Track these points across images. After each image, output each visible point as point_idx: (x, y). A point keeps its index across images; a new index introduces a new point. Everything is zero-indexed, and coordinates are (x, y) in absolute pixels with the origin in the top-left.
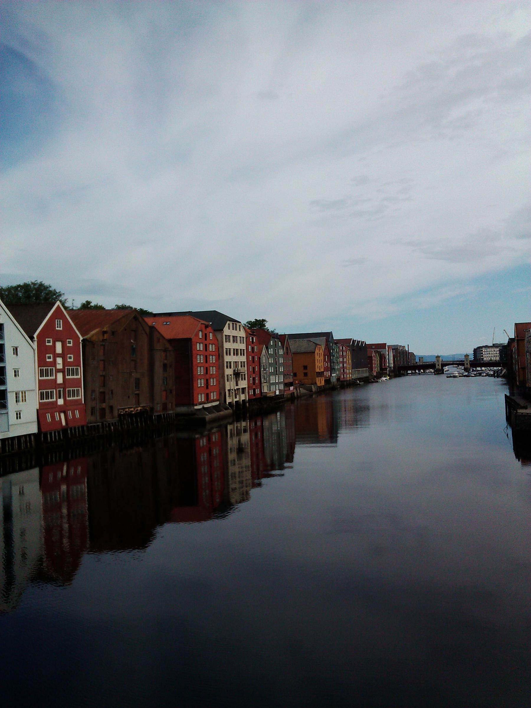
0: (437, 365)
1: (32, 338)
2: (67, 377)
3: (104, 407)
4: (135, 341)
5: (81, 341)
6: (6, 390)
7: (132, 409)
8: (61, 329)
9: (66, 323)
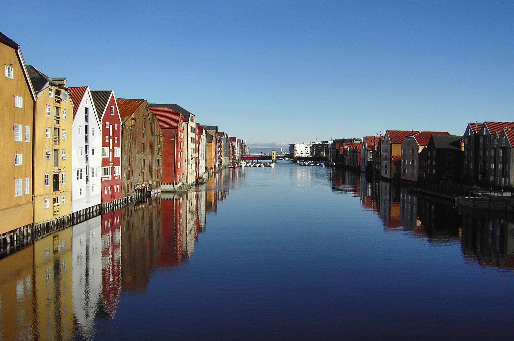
0: (272, 157)
1: (100, 121)
2: (115, 156)
4: (144, 127)
5: (121, 126)
8: (113, 115)
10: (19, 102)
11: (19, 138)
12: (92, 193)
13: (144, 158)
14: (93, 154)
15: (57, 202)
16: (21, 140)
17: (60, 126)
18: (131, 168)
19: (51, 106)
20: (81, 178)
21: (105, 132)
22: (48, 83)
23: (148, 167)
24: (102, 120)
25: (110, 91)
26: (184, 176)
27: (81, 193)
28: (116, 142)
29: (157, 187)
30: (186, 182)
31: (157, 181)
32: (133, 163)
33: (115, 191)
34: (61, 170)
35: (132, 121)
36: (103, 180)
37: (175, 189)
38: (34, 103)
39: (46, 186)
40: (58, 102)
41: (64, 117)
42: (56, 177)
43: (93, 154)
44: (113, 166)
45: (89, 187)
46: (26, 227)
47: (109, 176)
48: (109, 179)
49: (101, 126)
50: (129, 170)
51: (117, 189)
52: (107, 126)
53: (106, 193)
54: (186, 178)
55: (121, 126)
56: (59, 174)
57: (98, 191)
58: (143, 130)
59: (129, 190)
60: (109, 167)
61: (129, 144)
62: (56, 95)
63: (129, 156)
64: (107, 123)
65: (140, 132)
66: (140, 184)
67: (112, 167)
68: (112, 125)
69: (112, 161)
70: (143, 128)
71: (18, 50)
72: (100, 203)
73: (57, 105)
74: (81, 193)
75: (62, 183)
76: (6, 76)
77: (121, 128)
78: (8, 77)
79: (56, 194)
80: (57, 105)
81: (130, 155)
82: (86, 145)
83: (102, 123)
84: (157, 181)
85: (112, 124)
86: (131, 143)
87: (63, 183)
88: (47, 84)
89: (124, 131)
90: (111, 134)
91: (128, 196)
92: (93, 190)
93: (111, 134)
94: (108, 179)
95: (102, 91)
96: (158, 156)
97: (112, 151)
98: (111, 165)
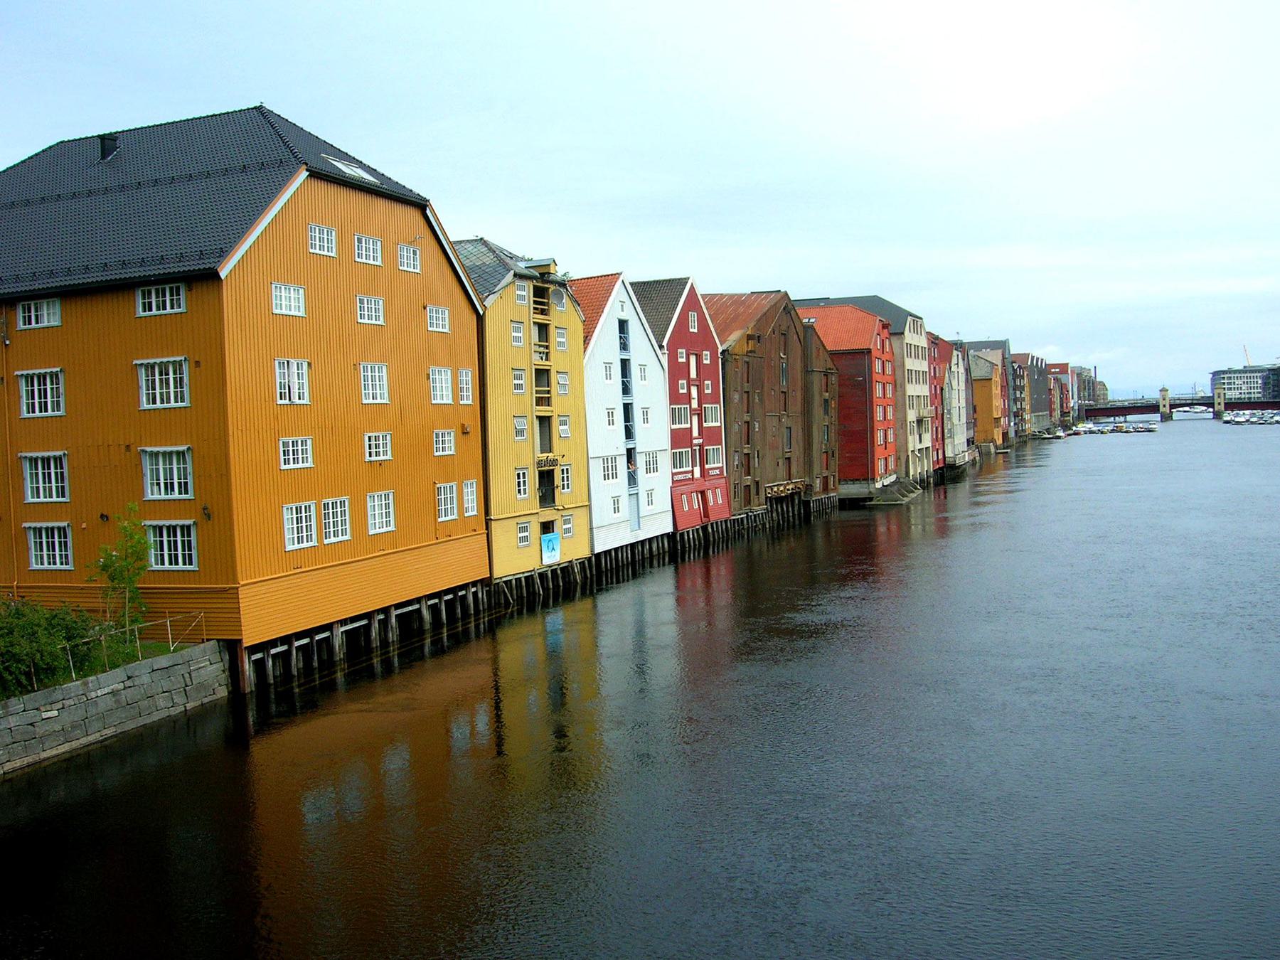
0: (1161, 407)
1: (661, 347)
2: (705, 425)
3: (749, 484)
4: (784, 354)
5: (719, 355)
6: (634, 449)
7: (782, 488)
8: (696, 331)
9: (702, 319)
10: (440, 321)
11: (443, 394)
12: (645, 509)
13: (789, 426)
14: (646, 420)
15: (551, 530)
16: (448, 400)
17: (551, 366)
18: (753, 448)
19: (523, 323)
20: (615, 476)
21: (676, 372)
22: (512, 272)
23: (801, 445)
24: (667, 344)
25: (685, 279)
26: (901, 464)
27: (616, 510)
28: (708, 391)
29: (825, 488)
30: (904, 476)
31: (826, 478)
32: (757, 437)
33: (711, 503)
34: (557, 460)
35: (748, 343)
36: (676, 478)
37: (870, 492)
38: (480, 319)
39: (519, 496)
40: (543, 312)
41: (560, 344)
42: (546, 478)
43: (646, 420)
44: (701, 446)
45: (638, 497)
46: (470, 586)
47: (693, 471)
48: (693, 475)
49: (665, 360)
50: (748, 454)
51: (717, 498)
52: (707, 359)
53: (686, 509)
54: (904, 466)
55: (719, 355)
56: (553, 470)
57: (663, 502)
58: (782, 361)
59: (752, 498)
60: (694, 451)
61: (746, 395)
62: (534, 297)
63: (748, 422)
64: (682, 351)
65: (775, 365)
66: (781, 485)
67: (699, 450)
68: (696, 355)
69: (699, 435)
70: (782, 355)
71: (426, 210)
72: (670, 529)
73: (541, 319)
74: (616, 510)
75: (563, 489)
76: (401, 268)
77: (720, 360)
78: (405, 268)
79: (548, 514)
80: (541, 319)
81: (747, 418)
82: (625, 402)
83: (667, 352)
84: (827, 477)
85: (696, 352)
86: (751, 393)
87: (566, 490)
88: (510, 277)
89: (728, 365)
90: (693, 374)
91: (750, 514)
92: (650, 503)
93: (693, 374)
94: (689, 476)
95: (670, 280)
96: (824, 418)
97: (701, 414)
98: (696, 445)
